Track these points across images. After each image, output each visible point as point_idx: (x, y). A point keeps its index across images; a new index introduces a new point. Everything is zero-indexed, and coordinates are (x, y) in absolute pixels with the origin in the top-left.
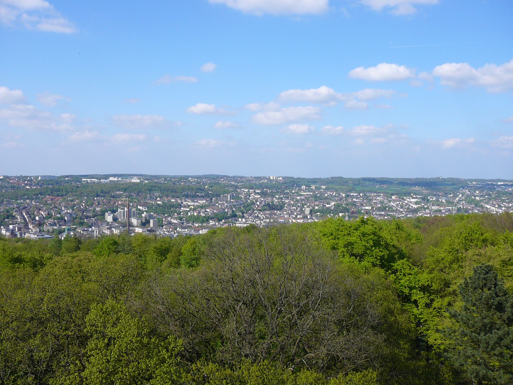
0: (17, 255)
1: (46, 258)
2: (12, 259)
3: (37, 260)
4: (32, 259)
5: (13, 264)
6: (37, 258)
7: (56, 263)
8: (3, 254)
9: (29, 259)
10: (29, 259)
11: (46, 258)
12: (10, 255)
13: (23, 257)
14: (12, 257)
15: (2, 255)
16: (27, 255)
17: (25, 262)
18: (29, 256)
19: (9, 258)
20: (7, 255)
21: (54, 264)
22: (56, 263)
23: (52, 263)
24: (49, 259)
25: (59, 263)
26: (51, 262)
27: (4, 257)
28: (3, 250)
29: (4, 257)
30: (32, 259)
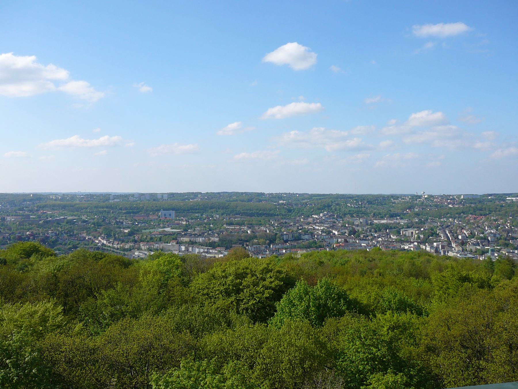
0: (464, 275)
1: (493, 280)
2: (460, 278)
3: (484, 281)
4: (480, 279)
5: (462, 283)
6: (483, 278)
7: (505, 286)
8: (452, 272)
9: (477, 279)
10: (477, 279)
11: (493, 280)
12: (459, 273)
13: (470, 277)
14: (461, 275)
15: (451, 273)
16: (474, 275)
17: (473, 282)
18: (477, 276)
19: (458, 276)
20: (456, 273)
21: (502, 286)
22: (505, 286)
23: (500, 287)
24: (496, 281)
25: (508, 286)
26: (500, 285)
27: (453, 275)
28: (452, 268)
29: (453, 275)
30: (480, 279)
